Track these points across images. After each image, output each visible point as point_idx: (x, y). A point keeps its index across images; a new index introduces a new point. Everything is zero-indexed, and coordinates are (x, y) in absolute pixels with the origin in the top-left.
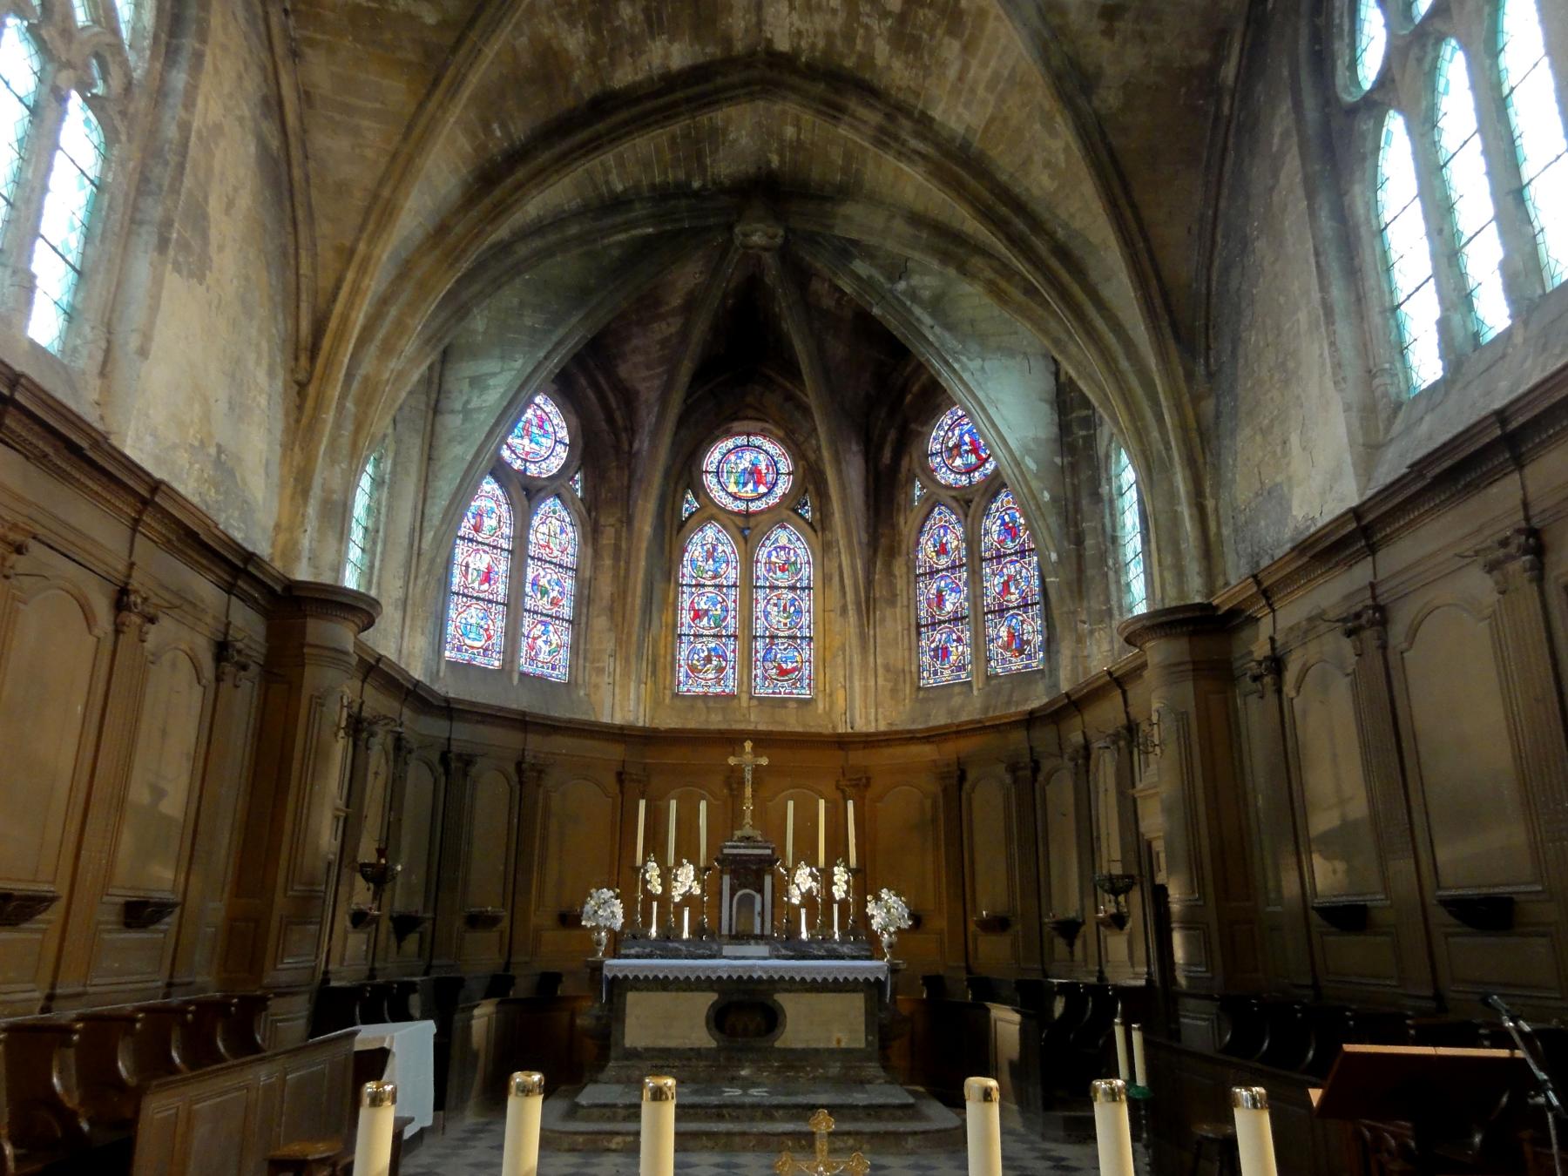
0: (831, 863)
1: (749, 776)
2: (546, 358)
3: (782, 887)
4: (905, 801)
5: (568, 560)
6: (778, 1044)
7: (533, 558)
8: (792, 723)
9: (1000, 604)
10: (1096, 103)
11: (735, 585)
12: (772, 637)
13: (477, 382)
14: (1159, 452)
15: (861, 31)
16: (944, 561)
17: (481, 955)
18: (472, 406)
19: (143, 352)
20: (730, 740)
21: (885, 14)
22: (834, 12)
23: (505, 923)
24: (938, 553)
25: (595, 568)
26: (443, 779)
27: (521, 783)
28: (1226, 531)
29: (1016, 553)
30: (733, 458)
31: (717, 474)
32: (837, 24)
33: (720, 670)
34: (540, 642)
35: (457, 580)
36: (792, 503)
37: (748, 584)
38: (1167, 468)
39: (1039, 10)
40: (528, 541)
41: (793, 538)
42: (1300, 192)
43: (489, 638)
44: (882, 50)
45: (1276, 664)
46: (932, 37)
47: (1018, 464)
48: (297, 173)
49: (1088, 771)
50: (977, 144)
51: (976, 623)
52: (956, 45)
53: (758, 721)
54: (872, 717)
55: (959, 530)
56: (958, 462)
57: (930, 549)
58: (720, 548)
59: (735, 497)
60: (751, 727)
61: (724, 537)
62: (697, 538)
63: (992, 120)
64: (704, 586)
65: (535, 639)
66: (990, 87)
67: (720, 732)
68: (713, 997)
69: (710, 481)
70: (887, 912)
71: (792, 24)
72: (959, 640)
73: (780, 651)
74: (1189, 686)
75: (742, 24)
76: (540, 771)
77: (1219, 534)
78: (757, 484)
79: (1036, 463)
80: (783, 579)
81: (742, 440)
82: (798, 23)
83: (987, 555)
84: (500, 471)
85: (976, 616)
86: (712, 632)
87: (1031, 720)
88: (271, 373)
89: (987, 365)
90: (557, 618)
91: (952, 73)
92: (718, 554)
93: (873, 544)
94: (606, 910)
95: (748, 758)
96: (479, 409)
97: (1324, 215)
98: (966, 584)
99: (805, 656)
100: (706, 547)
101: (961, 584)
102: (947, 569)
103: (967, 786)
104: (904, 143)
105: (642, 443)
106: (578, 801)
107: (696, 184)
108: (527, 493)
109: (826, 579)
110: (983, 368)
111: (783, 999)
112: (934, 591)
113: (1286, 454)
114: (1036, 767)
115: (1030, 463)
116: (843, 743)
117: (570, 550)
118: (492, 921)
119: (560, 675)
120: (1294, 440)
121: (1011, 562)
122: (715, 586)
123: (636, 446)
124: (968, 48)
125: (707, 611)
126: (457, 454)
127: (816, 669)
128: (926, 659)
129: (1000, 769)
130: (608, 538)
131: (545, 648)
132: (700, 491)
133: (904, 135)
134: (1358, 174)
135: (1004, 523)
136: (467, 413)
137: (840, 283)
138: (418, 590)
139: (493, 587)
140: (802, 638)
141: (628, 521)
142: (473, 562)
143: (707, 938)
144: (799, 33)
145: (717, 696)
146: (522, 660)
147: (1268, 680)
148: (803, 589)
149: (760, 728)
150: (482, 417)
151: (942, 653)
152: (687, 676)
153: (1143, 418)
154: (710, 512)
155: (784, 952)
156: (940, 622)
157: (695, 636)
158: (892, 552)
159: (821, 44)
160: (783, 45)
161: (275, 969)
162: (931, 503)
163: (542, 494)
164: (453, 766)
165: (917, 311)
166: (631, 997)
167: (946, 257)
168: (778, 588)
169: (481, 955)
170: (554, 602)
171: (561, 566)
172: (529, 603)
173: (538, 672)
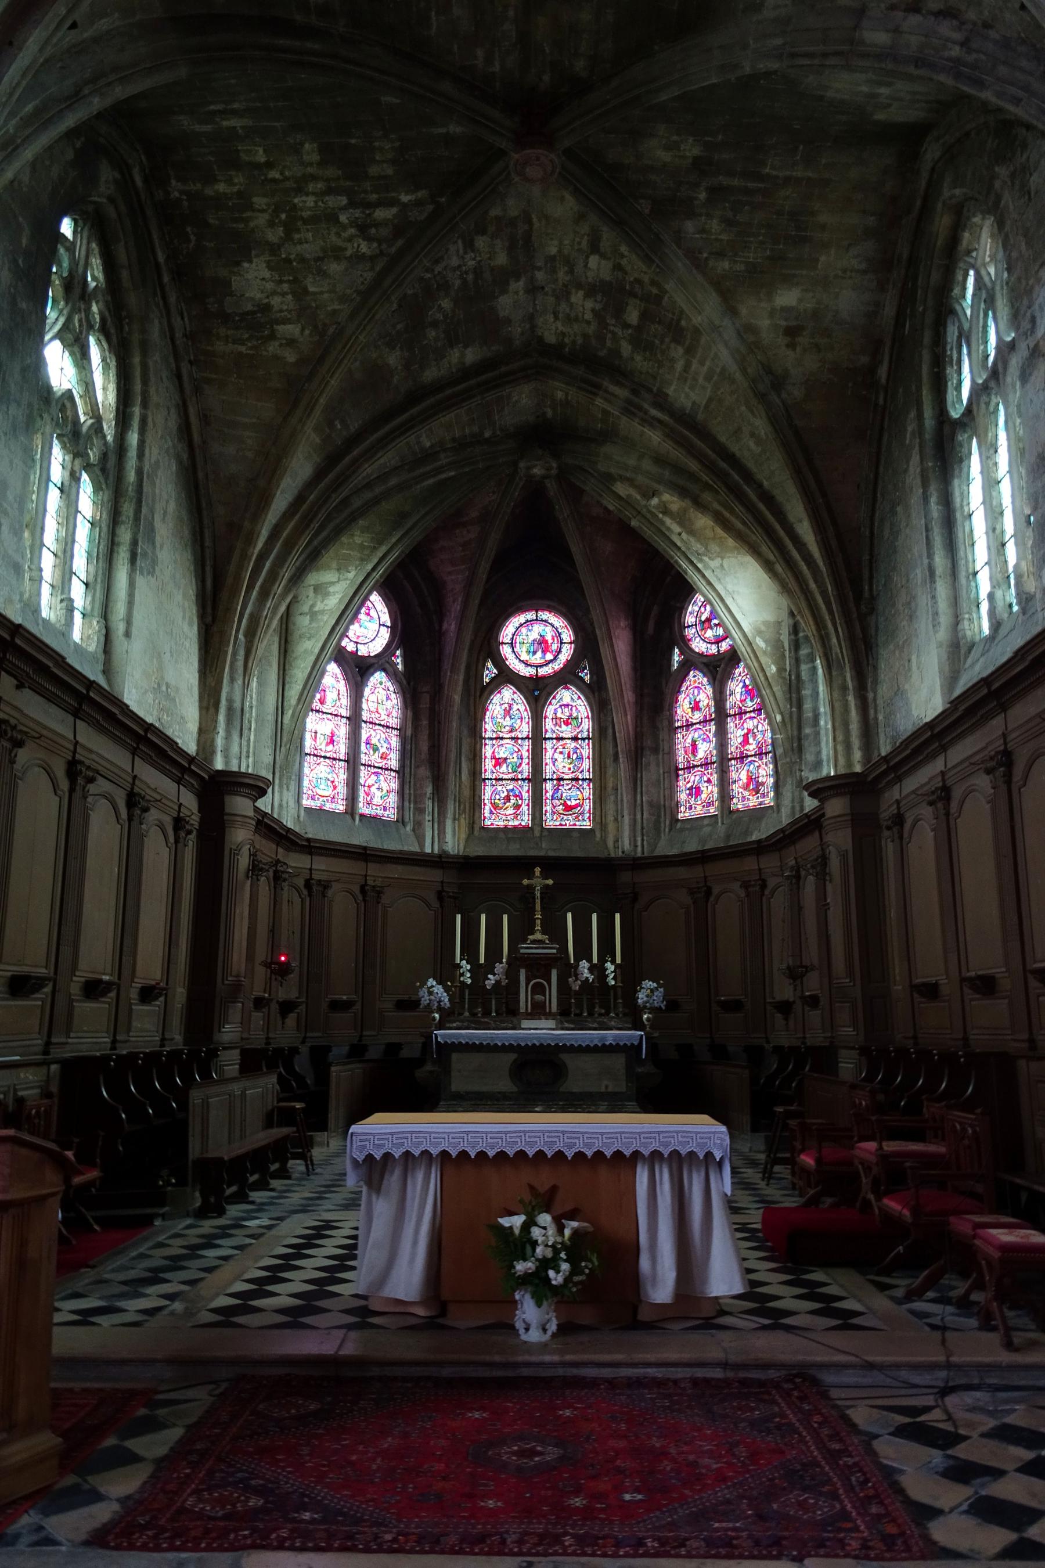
0: (602, 960)
1: (538, 894)
2: (374, 569)
5: (394, 722)
6: (561, 1090)
7: (366, 722)
9: (742, 753)
10: (784, 395)
11: (528, 738)
12: (559, 779)
13: (320, 590)
14: (836, 654)
15: (609, 335)
16: (697, 716)
18: (316, 609)
19: (127, 634)
20: (524, 865)
21: (626, 326)
22: (588, 323)
23: (358, 1007)
24: (693, 709)
25: (416, 727)
26: (308, 899)
27: (364, 900)
28: (881, 717)
29: (754, 711)
30: (524, 630)
31: (512, 644)
32: (591, 330)
33: (517, 807)
34: (373, 789)
35: (308, 744)
37: (537, 738)
38: (841, 668)
39: (739, 333)
40: (361, 709)
41: (575, 697)
42: (918, 481)
43: (335, 788)
44: (626, 349)
45: (899, 820)
46: (662, 342)
47: (750, 644)
48: (201, 475)
49: (799, 888)
50: (700, 417)
52: (680, 350)
53: (546, 849)
54: (639, 843)
55: (709, 690)
56: (709, 634)
57: (686, 705)
58: (515, 707)
59: (527, 664)
60: (542, 854)
61: (519, 698)
62: (496, 699)
63: (710, 400)
64: (502, 738)
65: (369, 787)
66: (708, 378)
67: (517, 858)
68: (513, 1056)
69: (506, 651)
71: (557, 328)
72: (709, 781)
74: (849, 830)
75: (519, 330)
76: (379, 892)
77: (876, 719)
78: (544, 652)
79: (765, 641)
80: (567, 731)
81: (531, 615)
82: (561, 328)
83: (732, 712)
84: (342, 657)
86: (510, 776)
88: (190, 624)
89: (726, 563)
90: (387, 769)
91: (679, 366)
92: (514, 712)
95: (538, 881)
96: (322, 612)
97: (933, 500)
98: (715, 735)
99: (586, 794)
101: (711, 735)
102: (700, 723)
103: (712, 899)
104: (646, 412)
105: (451, 626)
107: (487, 434)
108: (358, 670)
110: (722, 565)
111: (564, 1057)
112: (689, 741)
113: (910, 669)
114: (764, 885)
115: (760, 643)
117: (394, 714)
118: (346, 1006)
119: (391, 814)
120: (914, 659)
121: (751, 718)
122: (512, 738)
123: (445, 626)
124: (690, 351)
125: (506, 759)
126: (307, 648)
127: (594, 803)
128: (683, 796)
129: (736, 886)
130: (425, 703)
131: (378, 794)
133: (646, 406)
134: (956, 472)
135: (745, 686)
136: (313, 615)
137: (605, 502)
138: (282, 756)
140: (583, 780)
142: (322, 729)
144: (563, 334)
145: (515, 827)
146: (361, 805)
147: (895, 830)
148: (583, 739)
149: (551, 854)
150: (325, 618)
152: (491, 812)
153: (825, 627)
154: (506, 676)
155: (567, 1025)
156: (694, 766)
157: (496, 779)
159: (580, 341)
160: (551, 338)
161: (220, 1031)
162: (687, 666)
163: (372, 670)
165: (668, 521)
166: (455, 1056)
167: (683, 492)
168: (562, 739)
170: (384, 757)
171: (388, 727)
172: (364, 759)
173: (373, 813)
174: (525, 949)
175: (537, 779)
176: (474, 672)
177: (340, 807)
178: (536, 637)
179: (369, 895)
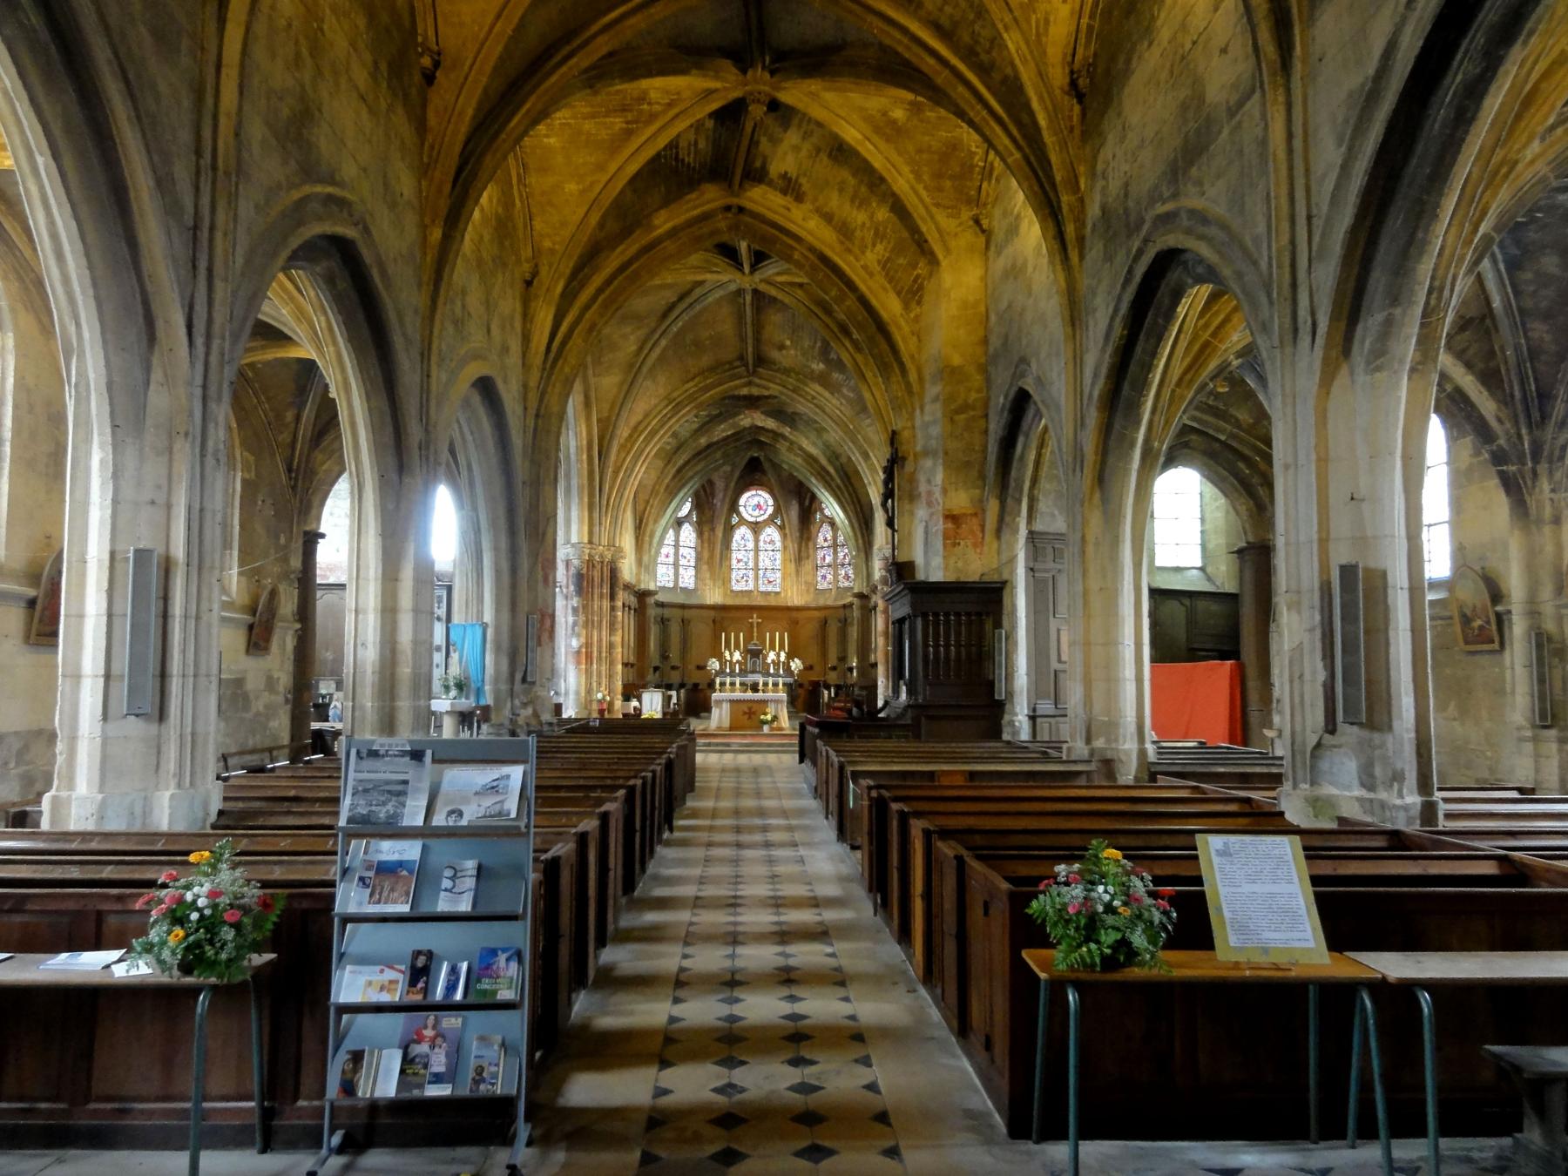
3: (765, 657)
4: (809, 630)
8: (773, 602)
17: (675, 677)
20: (752, 609)
36: (771, 520)
37: (757, 550)
51: (835, 569)
53: (761, 602)
69: (741, 509)
70: (796, 665)
73: (768, 574)
80: (770, 547)
85: (834, 566)
87: (844, 606)
93: (801, 537)
94: (714, 664)
95: (755, 619)
100: (742, 535)
106: (701, 630)
109: (785, 548)
116: (789, 609)
119: (692, 586)
132: (739, 514)
139: (673, 564)
141: (713, 530)
143: (743, 672)
151: (824, 577)
154: (743, 521)
158: (809, 539)
164: (663, 622)
169: (675, 677)
174: (751, 647)
175: (756, 568)
176: (729, 517)
177: (671, 585)
178: (756, 503)
179: (685, 622)
